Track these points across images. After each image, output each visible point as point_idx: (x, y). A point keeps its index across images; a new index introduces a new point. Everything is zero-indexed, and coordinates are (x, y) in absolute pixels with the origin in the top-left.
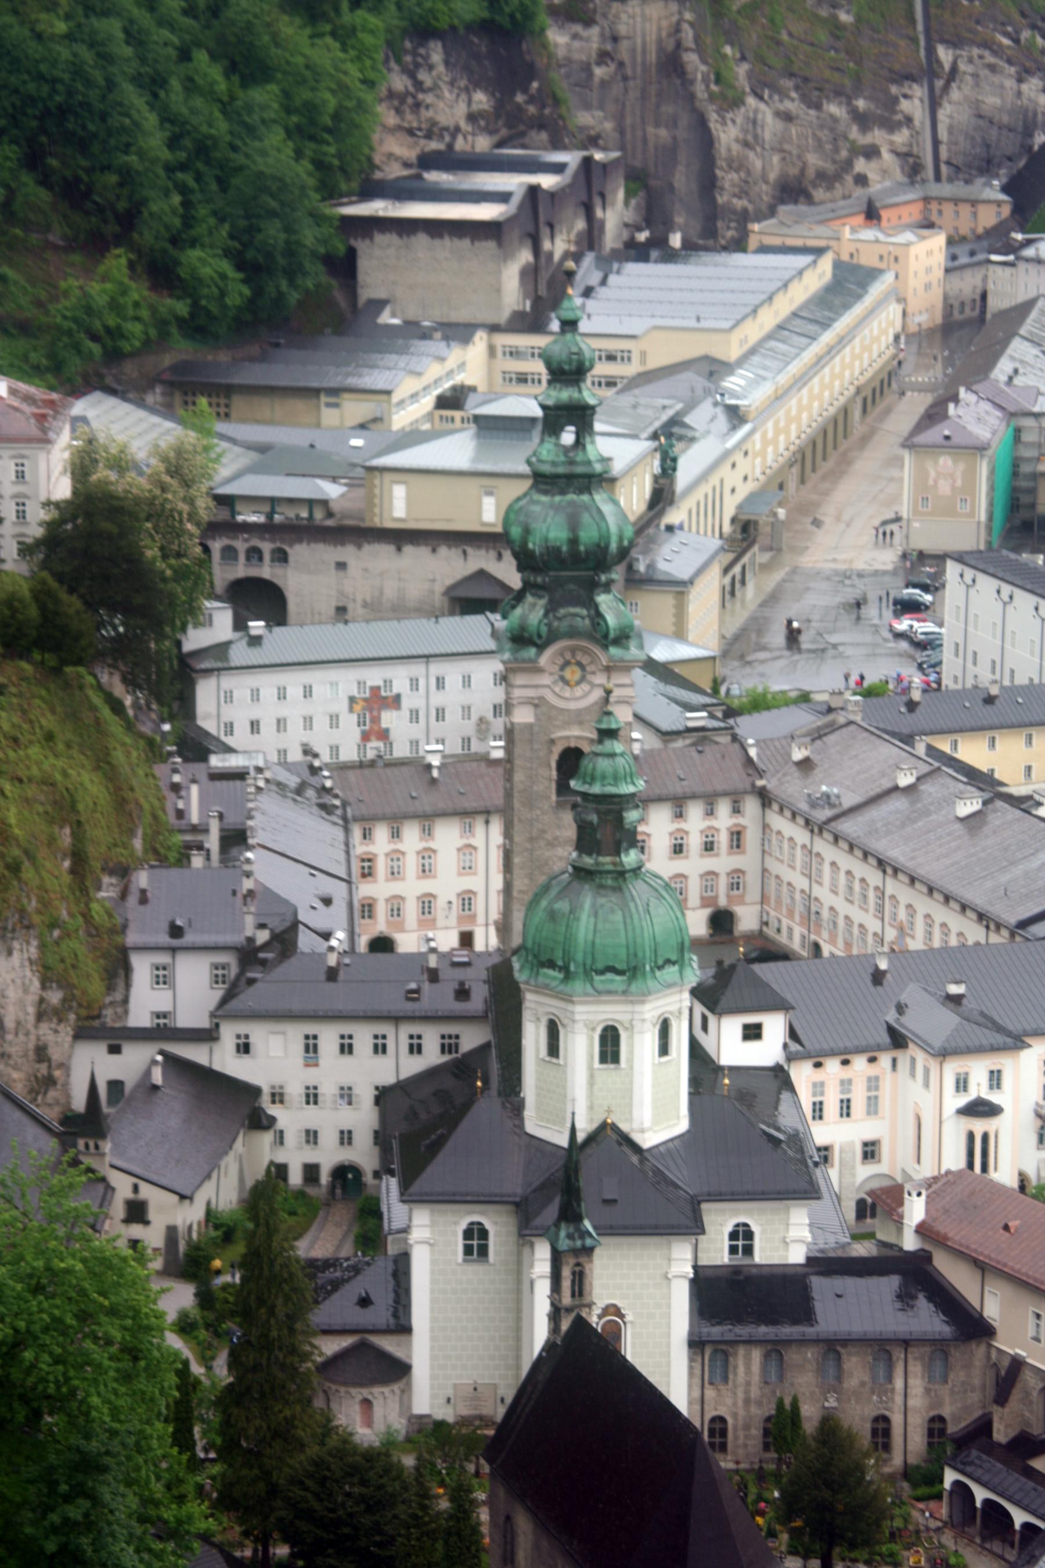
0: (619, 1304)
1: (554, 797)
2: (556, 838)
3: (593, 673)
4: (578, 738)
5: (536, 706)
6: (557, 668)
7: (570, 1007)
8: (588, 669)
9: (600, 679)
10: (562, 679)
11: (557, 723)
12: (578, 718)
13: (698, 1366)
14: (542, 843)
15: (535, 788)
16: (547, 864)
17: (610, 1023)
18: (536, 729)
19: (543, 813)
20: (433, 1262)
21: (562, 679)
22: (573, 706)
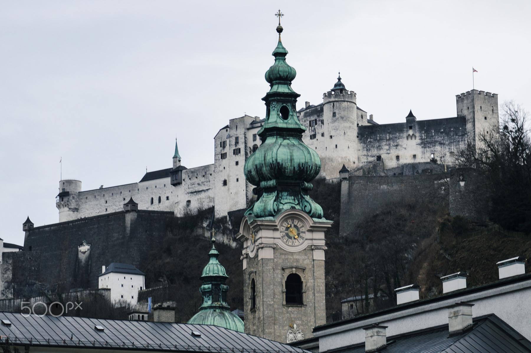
3: (304, 233)
5: (274, 248)
6: (284, 228)
8: (301, 230)
9: (308, 235)
10: (287, 235)
21: (287, 235)
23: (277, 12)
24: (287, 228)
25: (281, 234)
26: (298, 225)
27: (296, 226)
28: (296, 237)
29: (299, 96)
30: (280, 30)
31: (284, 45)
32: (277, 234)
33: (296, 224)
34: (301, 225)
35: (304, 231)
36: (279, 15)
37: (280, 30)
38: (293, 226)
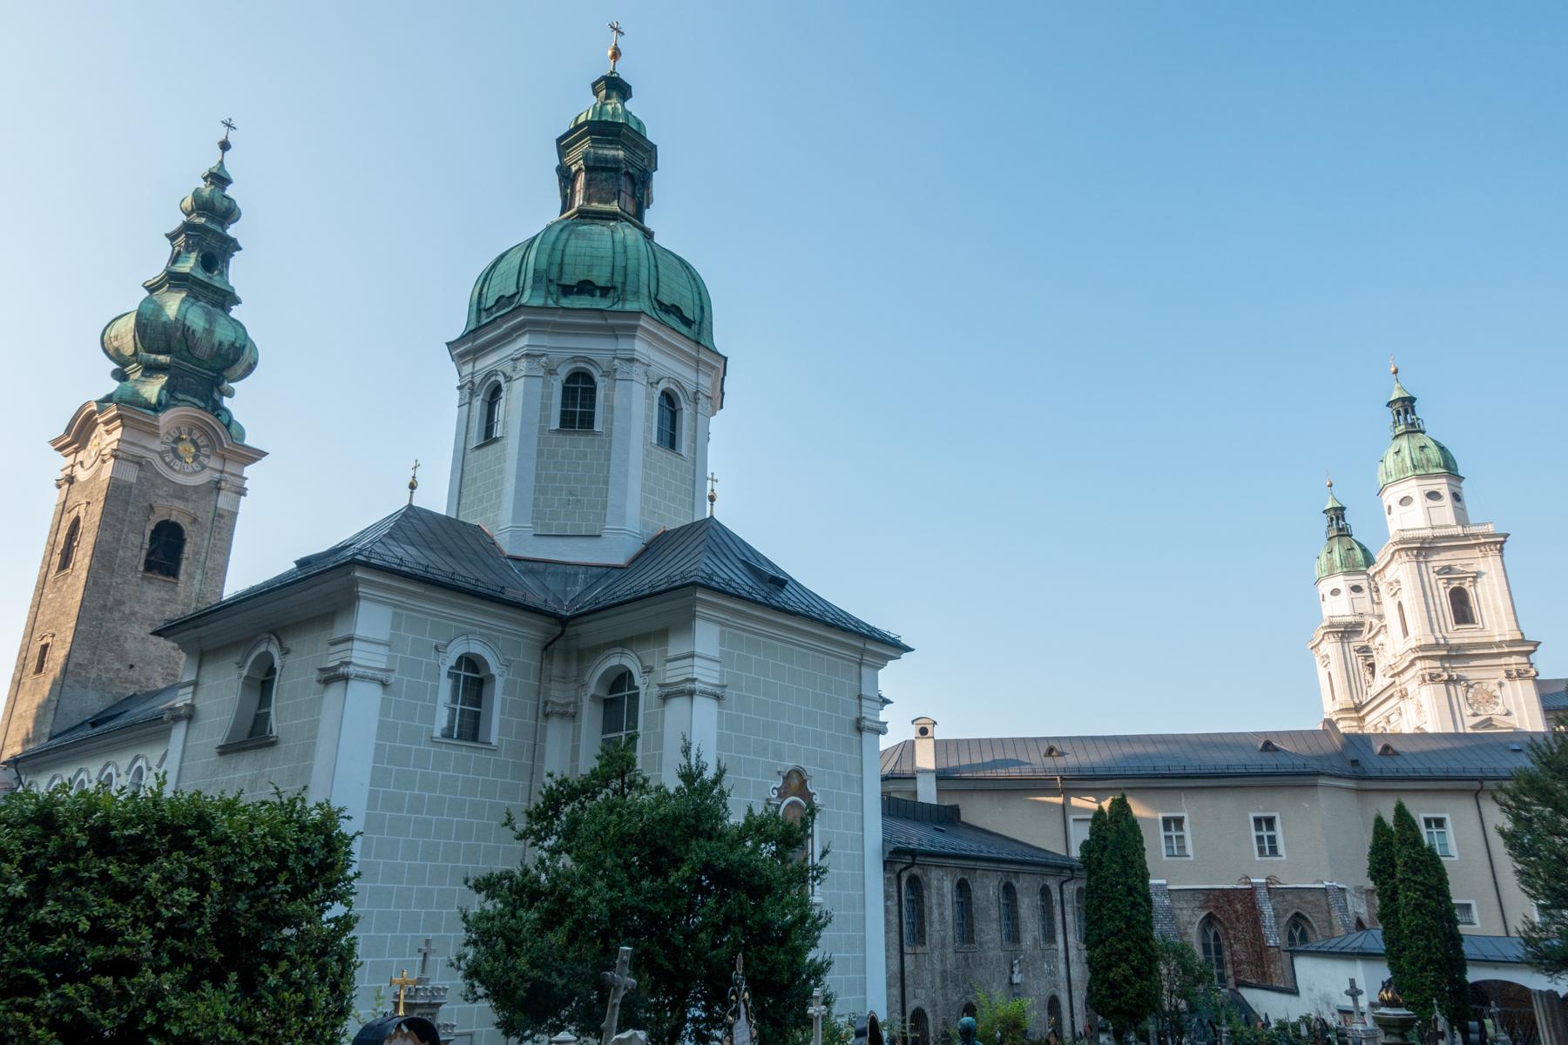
0: (810, 769)
1: (141, 568)
2: (134, 614)
3: (208, 457)
4: (181, 512)
6: (171, 439)
7: (623, 344)
9: (214, 463)
10: (174, 451)
11: (160, 493)
12: (182, 492)
13: (893, 904)
14: (117, 615)
15: (121, 553)
16: (117, 638)
17: (673, 387)
18: (135, 492)
19: (125, 583)
20: (384, 730)
22: (180, 479)
23: (226, 118)
24: (179, 440)
25: (163, 446)
26: (199, 441)
27: (194, 442)
28: (190, 460)
29: (239, 249)
30: (225, 146)
31: (227, 167)
32: (156, 445)
33: (195, 438)
34: (205, 443)
35: (208, 453)
36: (229, 126)
37: (225, 146)
38: (189, 439)
